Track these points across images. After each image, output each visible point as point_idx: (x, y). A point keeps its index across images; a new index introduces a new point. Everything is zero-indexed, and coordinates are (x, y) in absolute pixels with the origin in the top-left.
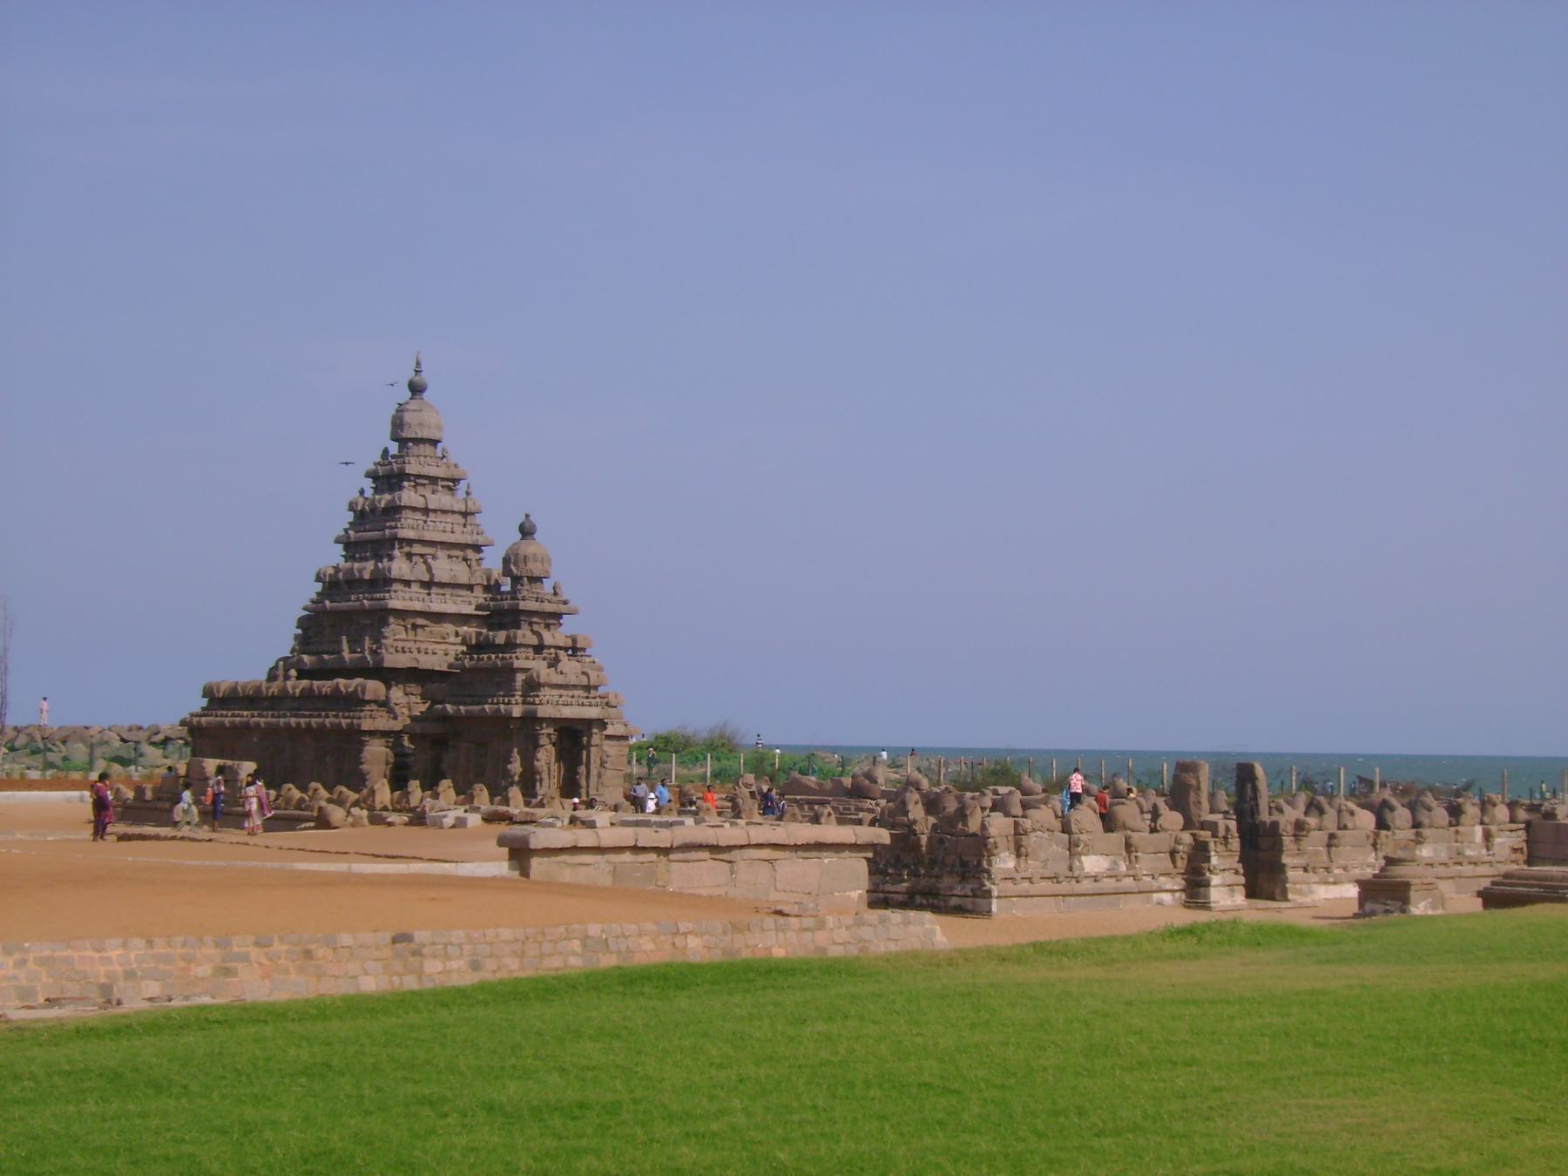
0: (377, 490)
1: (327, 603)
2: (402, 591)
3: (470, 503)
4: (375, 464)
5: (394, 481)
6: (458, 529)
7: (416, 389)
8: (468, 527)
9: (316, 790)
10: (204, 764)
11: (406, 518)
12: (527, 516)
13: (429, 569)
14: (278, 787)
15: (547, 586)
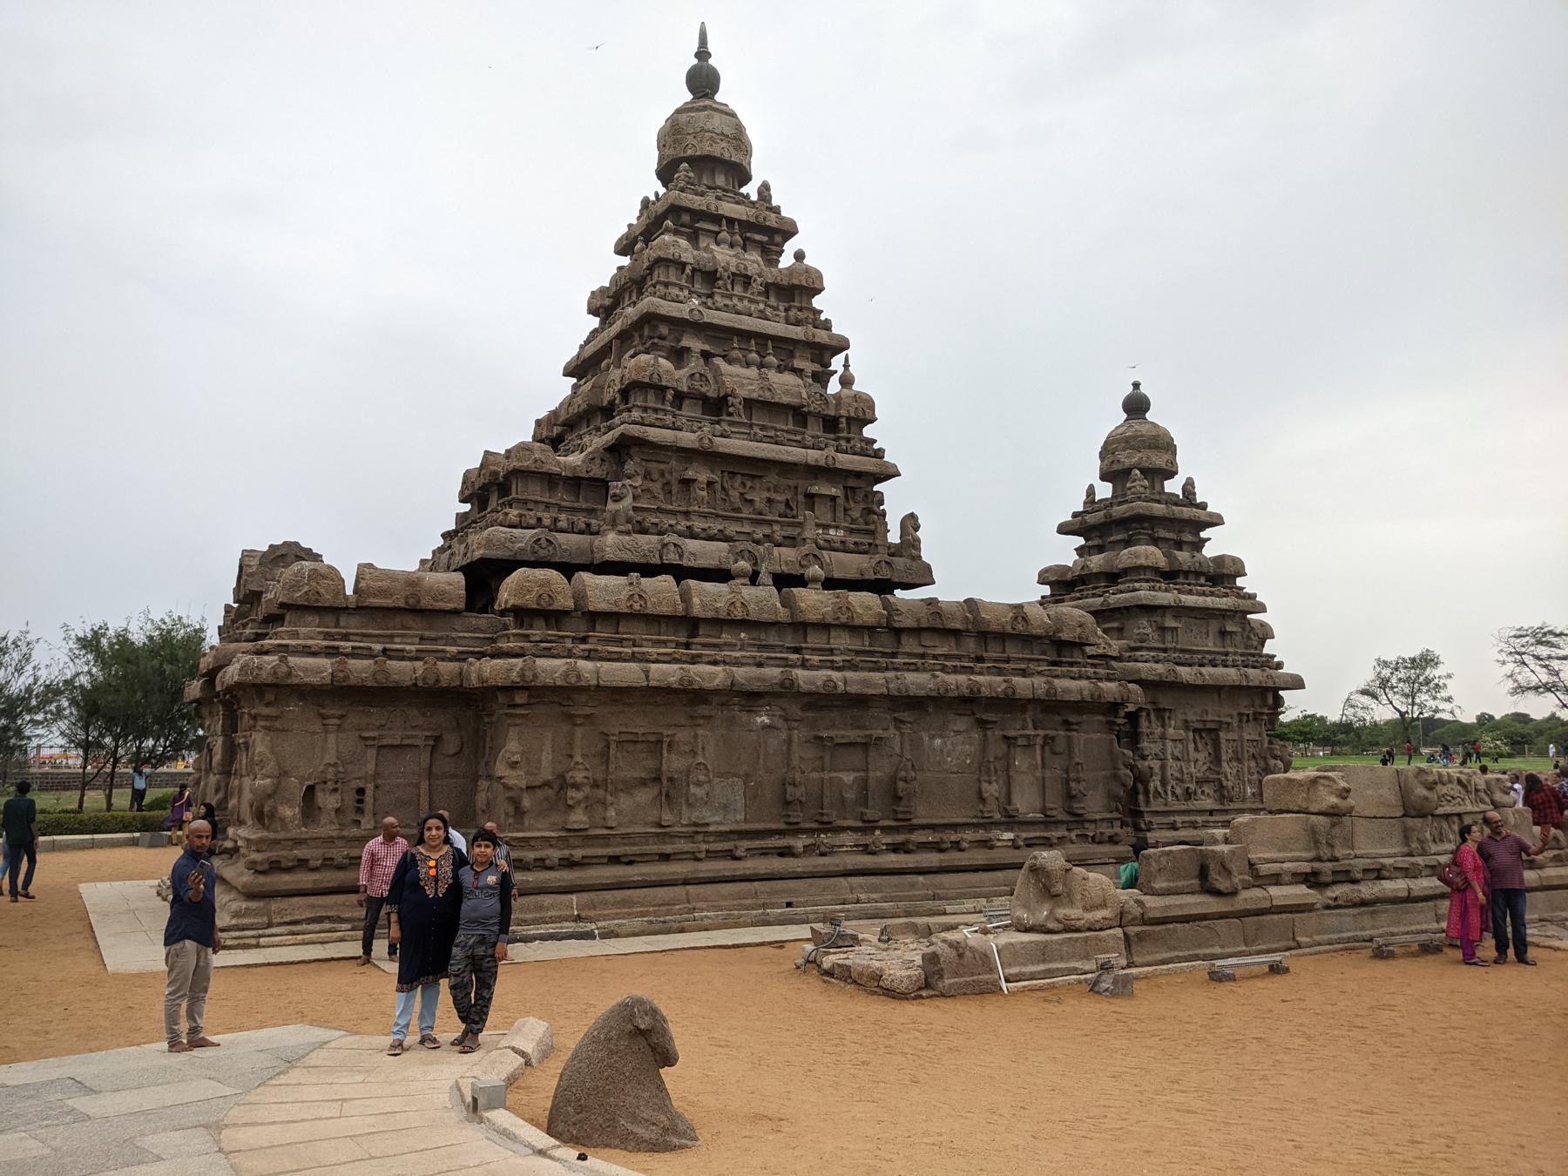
5: (758, 237)
12: (1136, 385)
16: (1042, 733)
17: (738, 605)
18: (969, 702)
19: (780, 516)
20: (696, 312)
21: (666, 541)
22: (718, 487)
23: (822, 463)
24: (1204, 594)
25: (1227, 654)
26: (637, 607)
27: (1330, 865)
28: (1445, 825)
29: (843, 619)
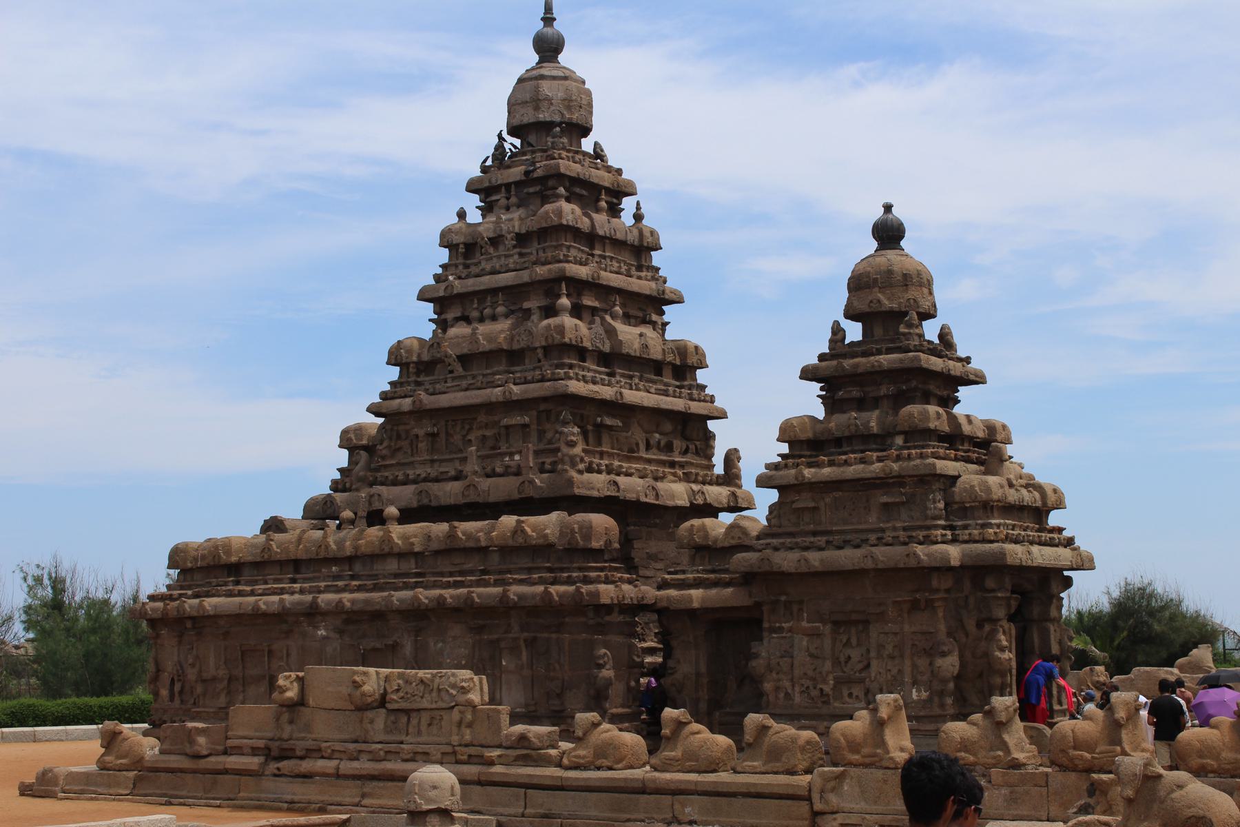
0: (486, 210)
1: (423, 396)
2: (580, 366)
3: (646, 234)
4: (484, 169)
5: (531, 190)
6: (633, 271)
7: (548, 47)
8: (644, 270)
9: (680, 725)
10: (357, 678)
11: (569, 248)
12: (888, 208)
13: (611, 332)
14: (560, 717)
15: (931, 330)
16: (526, 634)
17: (323, 547)
18: (465, 612)
19: (493, 448)
20: (449, 288)
21: (372, 493)
22: (443, 435)
23: (501, 399)
24: (846, 463)
25: (883, 530)
26: (266, 556)
27: (277, 743)
28: (404, 719)
29: (387, 550)
